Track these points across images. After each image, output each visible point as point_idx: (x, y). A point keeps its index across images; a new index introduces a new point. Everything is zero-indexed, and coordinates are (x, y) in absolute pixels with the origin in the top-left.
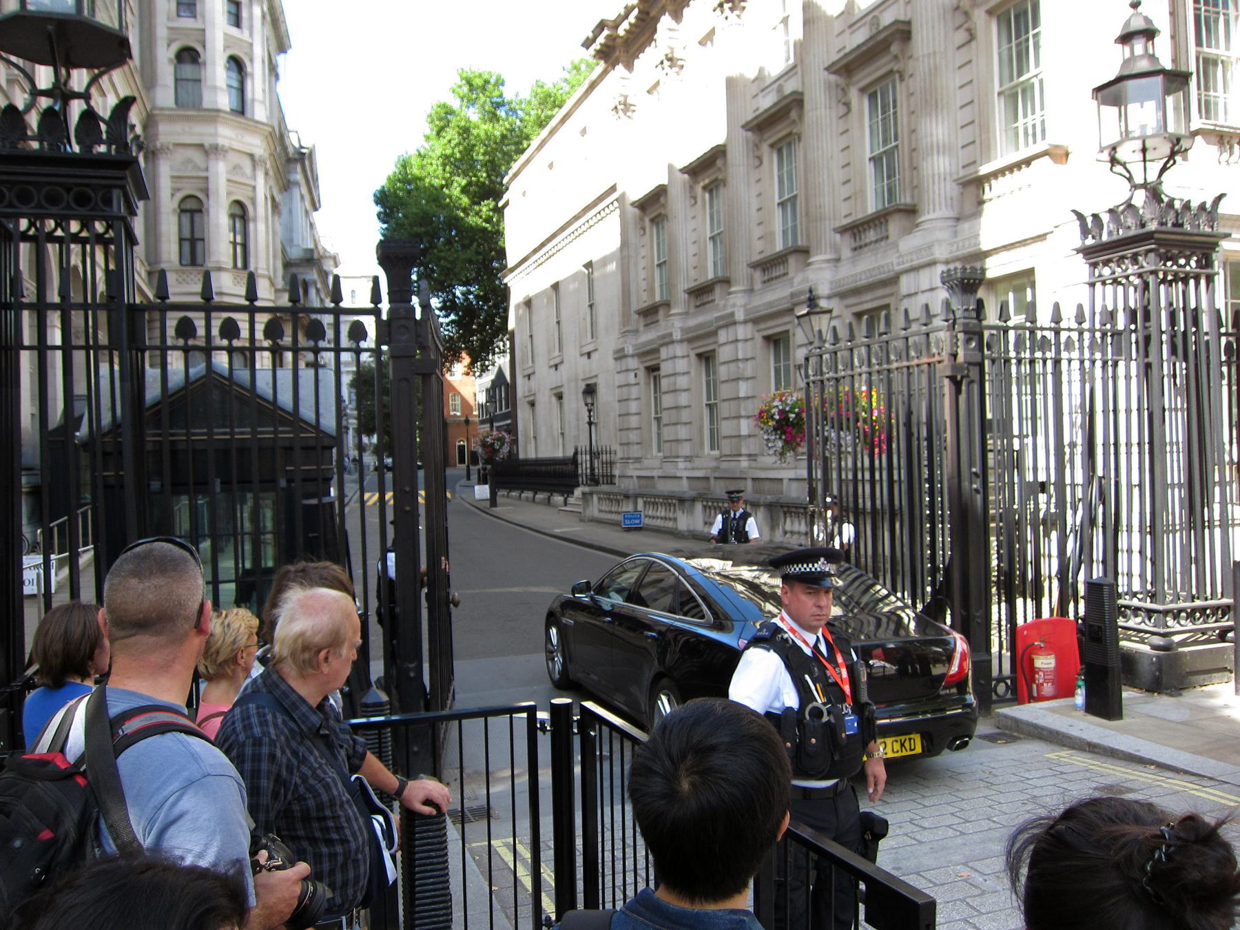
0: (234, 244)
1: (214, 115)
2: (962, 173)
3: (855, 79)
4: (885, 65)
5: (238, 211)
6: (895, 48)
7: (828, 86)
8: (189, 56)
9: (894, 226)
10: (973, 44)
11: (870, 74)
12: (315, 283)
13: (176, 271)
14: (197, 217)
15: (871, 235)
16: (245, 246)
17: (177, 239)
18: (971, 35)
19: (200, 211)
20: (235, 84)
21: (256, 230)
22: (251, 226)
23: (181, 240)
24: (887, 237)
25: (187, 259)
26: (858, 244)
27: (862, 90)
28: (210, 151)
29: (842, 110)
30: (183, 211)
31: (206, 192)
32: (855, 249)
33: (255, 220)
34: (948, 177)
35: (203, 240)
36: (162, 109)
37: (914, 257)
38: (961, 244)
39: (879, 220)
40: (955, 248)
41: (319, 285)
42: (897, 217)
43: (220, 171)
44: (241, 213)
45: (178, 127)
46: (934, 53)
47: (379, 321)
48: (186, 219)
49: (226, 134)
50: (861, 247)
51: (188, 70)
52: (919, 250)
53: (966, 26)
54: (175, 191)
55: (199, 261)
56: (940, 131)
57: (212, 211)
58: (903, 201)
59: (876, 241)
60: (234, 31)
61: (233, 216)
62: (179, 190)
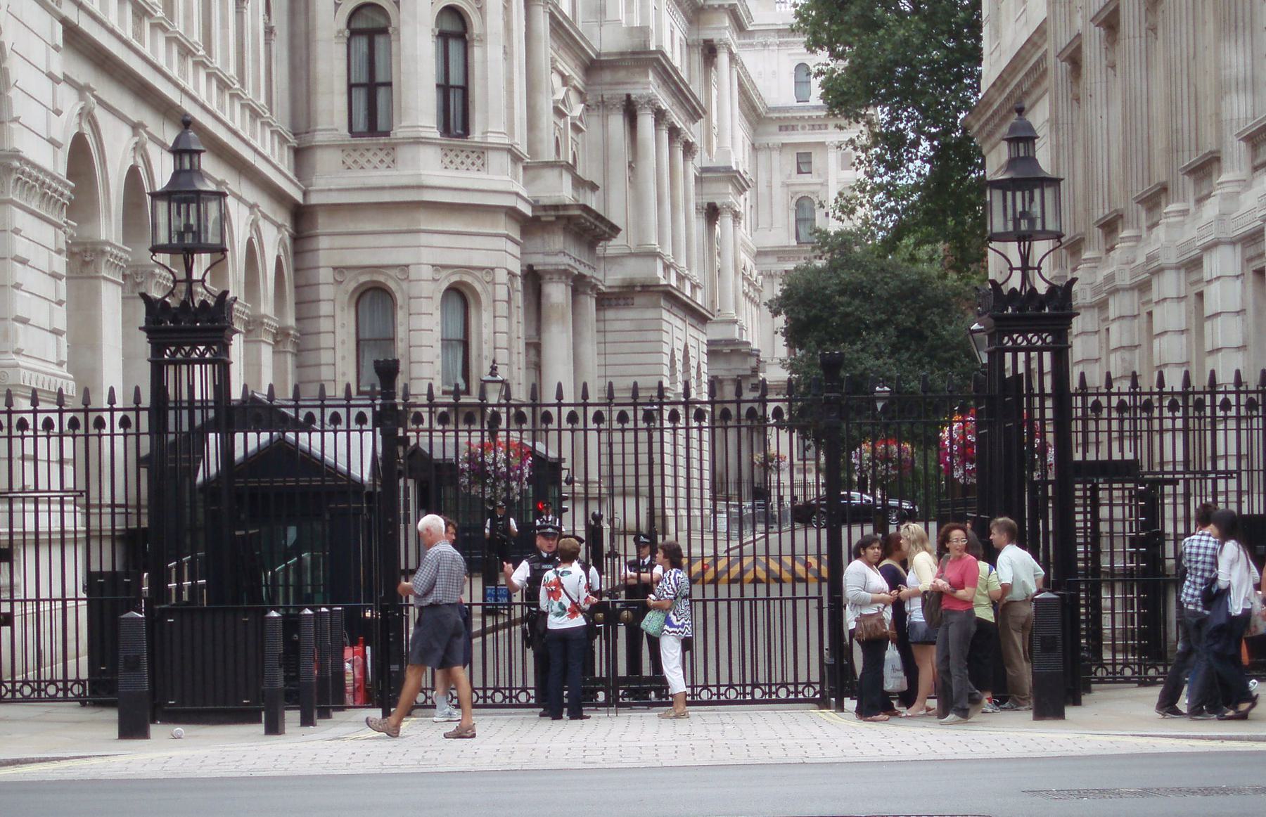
0: (444, 88)
5: (450, 26)
12: (651, 102)
13: (342, 147)
14: (380, 41)
16: (465, 90)
17: (344, 88)
19: (384, 31)
21: (485, 61)
22: (476, 53)
23: (351, 87)
25: (361, 124)
30: (354, 33)
33: (483, 40)
35: (389, 84)
41: (665, 102)
47: (374, 412)
48: (361, 44)
55: (381, 126)
57: (406, 32)
61: (443, 37)
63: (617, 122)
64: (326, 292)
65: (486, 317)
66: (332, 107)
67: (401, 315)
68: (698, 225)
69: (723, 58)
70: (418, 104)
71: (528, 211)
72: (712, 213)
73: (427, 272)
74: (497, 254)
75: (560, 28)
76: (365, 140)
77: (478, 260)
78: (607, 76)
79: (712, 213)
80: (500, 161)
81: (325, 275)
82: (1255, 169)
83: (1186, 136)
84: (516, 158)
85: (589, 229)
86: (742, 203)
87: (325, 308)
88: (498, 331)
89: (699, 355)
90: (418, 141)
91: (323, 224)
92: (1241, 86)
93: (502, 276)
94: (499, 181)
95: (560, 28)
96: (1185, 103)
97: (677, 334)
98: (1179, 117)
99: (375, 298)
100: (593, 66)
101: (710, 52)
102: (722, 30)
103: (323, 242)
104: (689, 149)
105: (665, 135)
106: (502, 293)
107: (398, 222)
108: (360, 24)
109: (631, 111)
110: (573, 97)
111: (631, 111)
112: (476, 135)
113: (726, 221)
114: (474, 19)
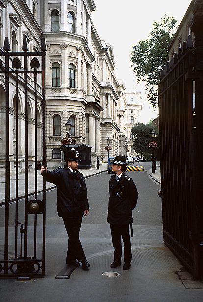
0: (70, 79)
1: (64, 34)
8: (56, 13)
16: (74, 79)
19: (59, 68)
20: (72, 22)
22: (76, 72)
23: (53, 78)
25: (55, 85)
28: (63, 46)
31: (61, 61)
36: (46, 32)
43: (66, 53)
44: (73, 67)
45: (52, 39)
49: (67, 40)
51: (54, 19)
54: (51, 60)
60: (71, 3)
62: (52, 60)
63: (105, 97)
64: (47, 116)
65: (78, 122)
66: (49, 82)
67: (61, 120)
68: (118, 118)
69: (121, 93)
70: (65, 82)
71: (86, 103)
72: (120, 116)
73: (67, 113)
74: (80, 110)
75: (93, 77)
76: (55, 88)
77: (76, 111)
78: (103, 90)
79: (120, 116)
80: (80, 93)
81: (48, 113)
84: (84, 93)
85: (99, 109)
86: (124, 115)
87: (47, 119)
88: (80, 124)
89: (117, 136)
90: (65, 88)
91: (47, 103)
93: (81, 114)
94: (80, 96)
95: (93, 77)
97: (114, 131)
99: (57, 117)
100: (101, 88)
101: (119, 93)
102: (121, 89)
103: (47, 107)
104: (116, 104)
105: (112, 100)
106: (81, 117)
107: (61, 103)
108: (55, 66)
109: (107, 96)
110: (98, 93)
111: (107, 96)
112: (76, 88)
113: (122, 117)
114: (76, 66)
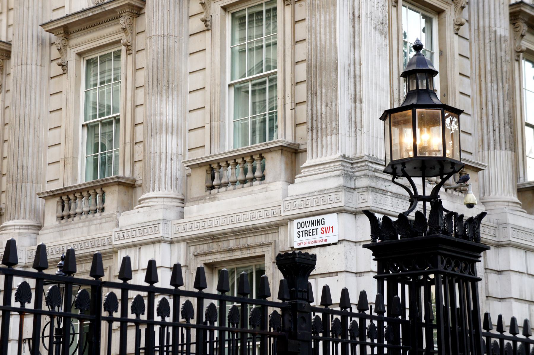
2: (189, 156)
3: (73, 42)
4: (110, 35)
6: (123, 21)
7: (42, 43)
9: (112, 198)
10: (208, 34)
11: (93, 40)
15: (83, 205)
18: (206, 26)
24: (103, 210)
26: (65, 213)
27: (80, 55)
29: (57, 70)
32: (62, 218)
34: (174, 158)
37: (137, 233)
38: (188, 226)
39: (95, 190)
40: (182, 227)
42: (116, 188)
46: (169, 34)
50: (69, 216)
52: (143, 227)
53: (203, 16)
56: (170, 112)
58: (120, 174)
59: (88, 212)
82: (212, 187)
83: (30, 171)
92: (170, 130)
96: (31, 149)
98: (25, 158)
